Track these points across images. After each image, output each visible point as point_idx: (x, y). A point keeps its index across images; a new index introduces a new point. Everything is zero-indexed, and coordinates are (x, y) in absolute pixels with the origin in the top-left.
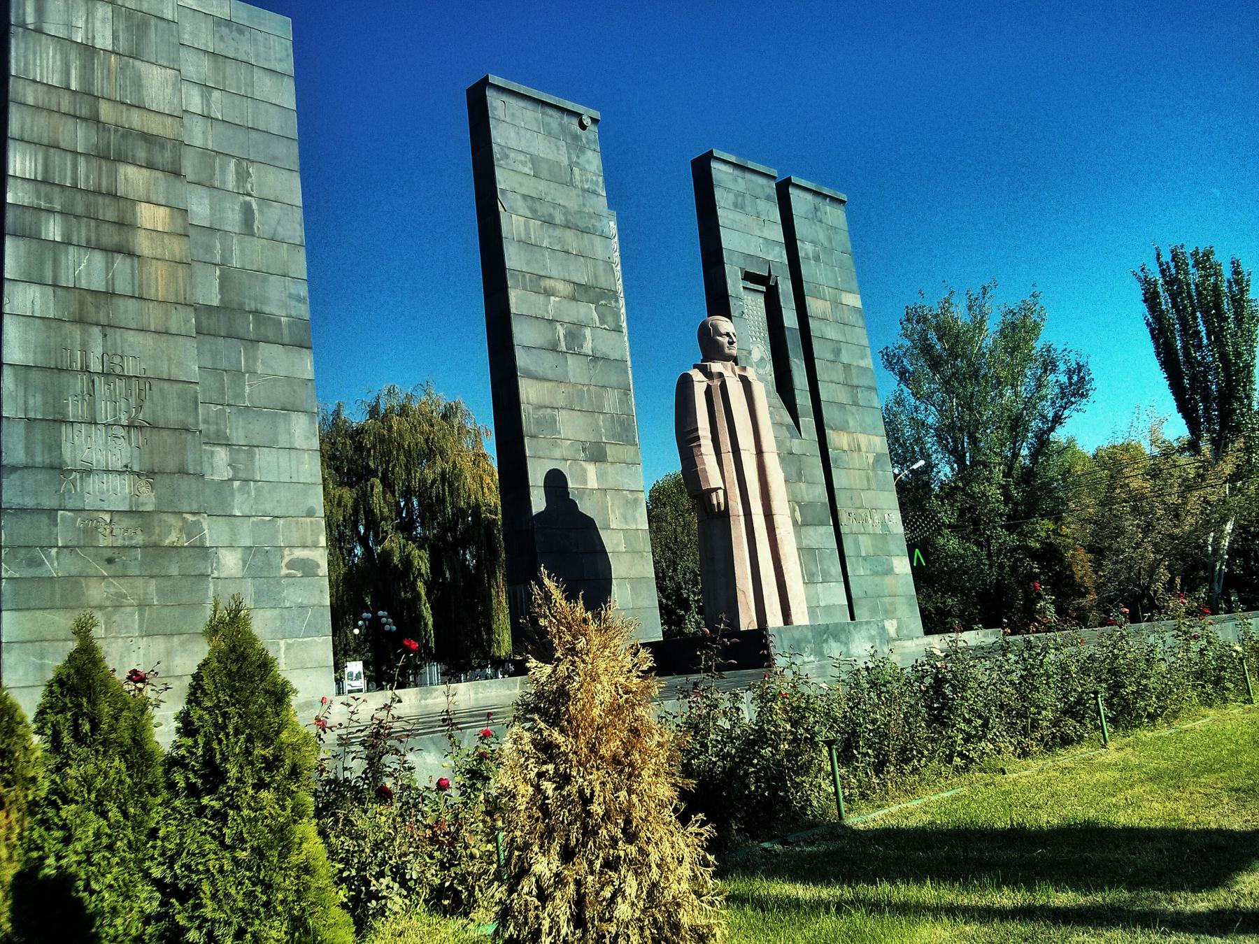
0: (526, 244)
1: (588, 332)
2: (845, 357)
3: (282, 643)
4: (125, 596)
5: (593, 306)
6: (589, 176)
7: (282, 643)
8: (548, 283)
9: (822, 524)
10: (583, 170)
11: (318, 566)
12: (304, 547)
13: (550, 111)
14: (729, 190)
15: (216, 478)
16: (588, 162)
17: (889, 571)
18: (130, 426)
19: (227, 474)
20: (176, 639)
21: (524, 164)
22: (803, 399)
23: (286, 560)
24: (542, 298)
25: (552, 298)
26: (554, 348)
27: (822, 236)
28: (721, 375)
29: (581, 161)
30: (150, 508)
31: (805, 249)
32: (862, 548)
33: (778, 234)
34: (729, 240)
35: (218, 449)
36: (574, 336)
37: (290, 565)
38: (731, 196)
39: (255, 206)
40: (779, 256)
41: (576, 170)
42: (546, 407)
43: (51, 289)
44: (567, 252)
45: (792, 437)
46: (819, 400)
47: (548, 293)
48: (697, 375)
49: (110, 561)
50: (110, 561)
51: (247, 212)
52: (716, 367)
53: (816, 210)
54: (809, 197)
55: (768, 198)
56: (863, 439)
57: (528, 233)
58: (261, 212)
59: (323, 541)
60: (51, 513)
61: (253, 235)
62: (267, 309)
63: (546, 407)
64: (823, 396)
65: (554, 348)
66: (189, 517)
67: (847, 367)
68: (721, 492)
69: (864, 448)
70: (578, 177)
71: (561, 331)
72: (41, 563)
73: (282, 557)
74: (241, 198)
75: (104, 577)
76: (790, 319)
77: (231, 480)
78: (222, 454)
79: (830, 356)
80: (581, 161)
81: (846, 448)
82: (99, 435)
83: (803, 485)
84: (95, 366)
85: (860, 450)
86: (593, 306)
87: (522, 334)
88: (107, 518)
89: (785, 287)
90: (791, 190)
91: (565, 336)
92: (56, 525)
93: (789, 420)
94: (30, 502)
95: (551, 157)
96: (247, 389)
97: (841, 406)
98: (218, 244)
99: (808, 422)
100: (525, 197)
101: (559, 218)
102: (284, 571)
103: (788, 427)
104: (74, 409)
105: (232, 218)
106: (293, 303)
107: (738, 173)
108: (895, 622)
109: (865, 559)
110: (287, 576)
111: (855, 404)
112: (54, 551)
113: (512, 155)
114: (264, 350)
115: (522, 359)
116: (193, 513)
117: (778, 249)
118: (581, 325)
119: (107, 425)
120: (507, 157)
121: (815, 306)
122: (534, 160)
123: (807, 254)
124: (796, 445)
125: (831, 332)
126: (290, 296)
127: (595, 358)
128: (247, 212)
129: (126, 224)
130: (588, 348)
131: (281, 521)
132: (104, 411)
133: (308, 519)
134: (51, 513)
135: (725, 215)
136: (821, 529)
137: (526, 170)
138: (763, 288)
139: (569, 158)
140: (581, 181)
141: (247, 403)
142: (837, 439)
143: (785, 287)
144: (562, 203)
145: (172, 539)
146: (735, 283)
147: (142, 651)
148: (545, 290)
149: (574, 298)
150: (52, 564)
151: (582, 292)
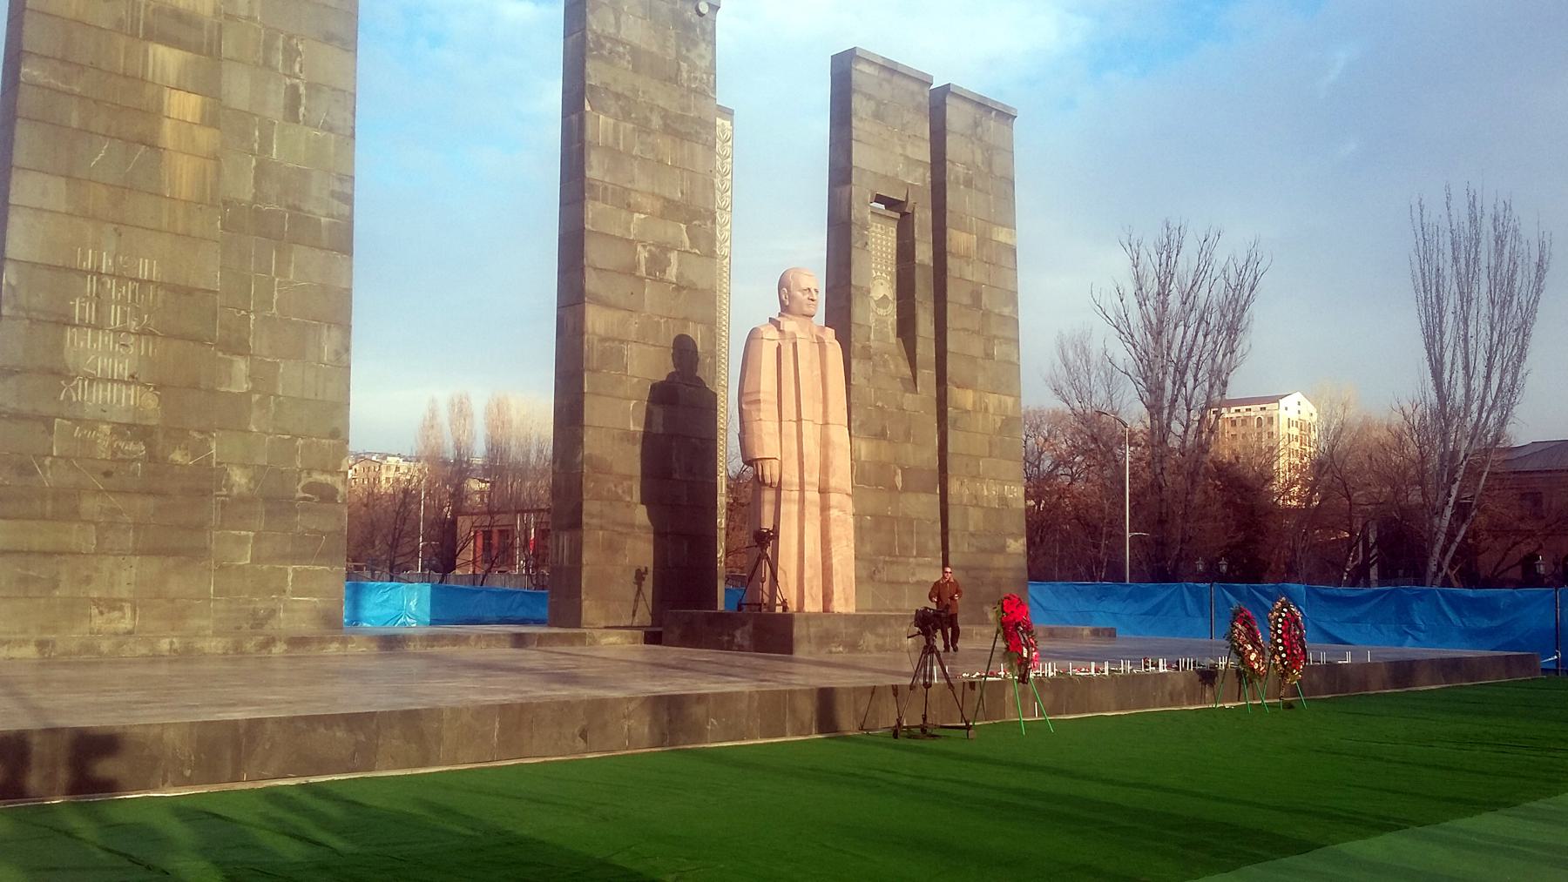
0: (614, 153)
1: (673, 256)
4: (120, 512)
5: (683, 226)
6: (698, 74)
9: (926, 491)
10: (693, 68)
11: (337, 491)
12: (324, 471)
14: (869, 97)
15: (234, 390)
16: (702, 57)
17: (1002, 549)
18: (139, 334)
19: (246, 387)
20: (171, 561)
22: (925, 349)
24: (624, 214)
26: (630, 270)
27: (979, 158)
28: (794, 336)
29: (692, 55)
30: (153, 422)
31: (955, 171)
32: (971, 523)
33: (924, 153)
34: (862, 156)
36: (657, 264)
37: (309, 488)
38: (872, 104)
39: (302, 90)
40: (920, 178)
41: (684, 66)
42: (614, 340)
43: (63, 180)
44: (660, 162)
45: (906, 390)
46: (945, 351)
47: (630, 208)
48: (772, 333)
50: (107, 474)
52: (789, 325)
53: (976, 124)
54: (968, 107)
55: (918, 108)
56: (992, 400)
57: (616, 139)
58: (308, 97)
60: (47, 421)
61: (298, 122)
62: (306, 207)
63: (614, 340)
64: (950, 346)
66: (195, 434)
67: (987, 314)
68: (775, 463)
69: (991, 410)
70: (685, 75)
71: (643, 255)
73: (299, 480)
74: (288, 81)
76: (924, 253)
77: (248, 394)
78: (241, 366)
79: (966, 300)
80: (692, 55)
81: (969, 407)
82: (105, 339)
83: (910, 447)
84: (106, 264)
85: (986, 409)
86: (683, 226)
87: (594, 253)
88: (106, 428)
89: (923, 217)
90: (948, 100)
92: (51, 433)
93: (907, 372)
94: (26, 408)
95: (654, 49)
97: (973, 359)
99: (927, 374)
100: (618, 96)
101: (656, 121)
102: (300, 494)
103: (903, 380)
104: (81, 308)
105: (276, 103)
106: (336, 202)
107: (884, 75)
109: (972, 535)
110: (305, 499)
111: (989, 356)
112: (48, 461)
113: (608, 45)
114: (299, 254)
115: (592, 283)
116: (201, 432)
117: (921, 170)
118: (664, 248)
119: (115, 331)
120: (602, 46)
121: (958, 239)
123: (957, 178)
124: (909, 400)
125: (972, 273)
126: (333, 194)
127: (679, 288)
129: (154, 113)
130: (672, 273)
131: (300, 442)
132: (115, 315)
134: (47, 421)
135: (861, 126)
136: (924, 498)
138: (897, 216)
139: (678, 52)
140: (689, 79)
142: (962, 398)
143: (923, 217)
144: (661, 103)
145: (177, 456)
146: (864, 209)
147: (134, 570)
148: (629, 205)
149: (662, 216)
150: (44, 473)
151: (671, 210)
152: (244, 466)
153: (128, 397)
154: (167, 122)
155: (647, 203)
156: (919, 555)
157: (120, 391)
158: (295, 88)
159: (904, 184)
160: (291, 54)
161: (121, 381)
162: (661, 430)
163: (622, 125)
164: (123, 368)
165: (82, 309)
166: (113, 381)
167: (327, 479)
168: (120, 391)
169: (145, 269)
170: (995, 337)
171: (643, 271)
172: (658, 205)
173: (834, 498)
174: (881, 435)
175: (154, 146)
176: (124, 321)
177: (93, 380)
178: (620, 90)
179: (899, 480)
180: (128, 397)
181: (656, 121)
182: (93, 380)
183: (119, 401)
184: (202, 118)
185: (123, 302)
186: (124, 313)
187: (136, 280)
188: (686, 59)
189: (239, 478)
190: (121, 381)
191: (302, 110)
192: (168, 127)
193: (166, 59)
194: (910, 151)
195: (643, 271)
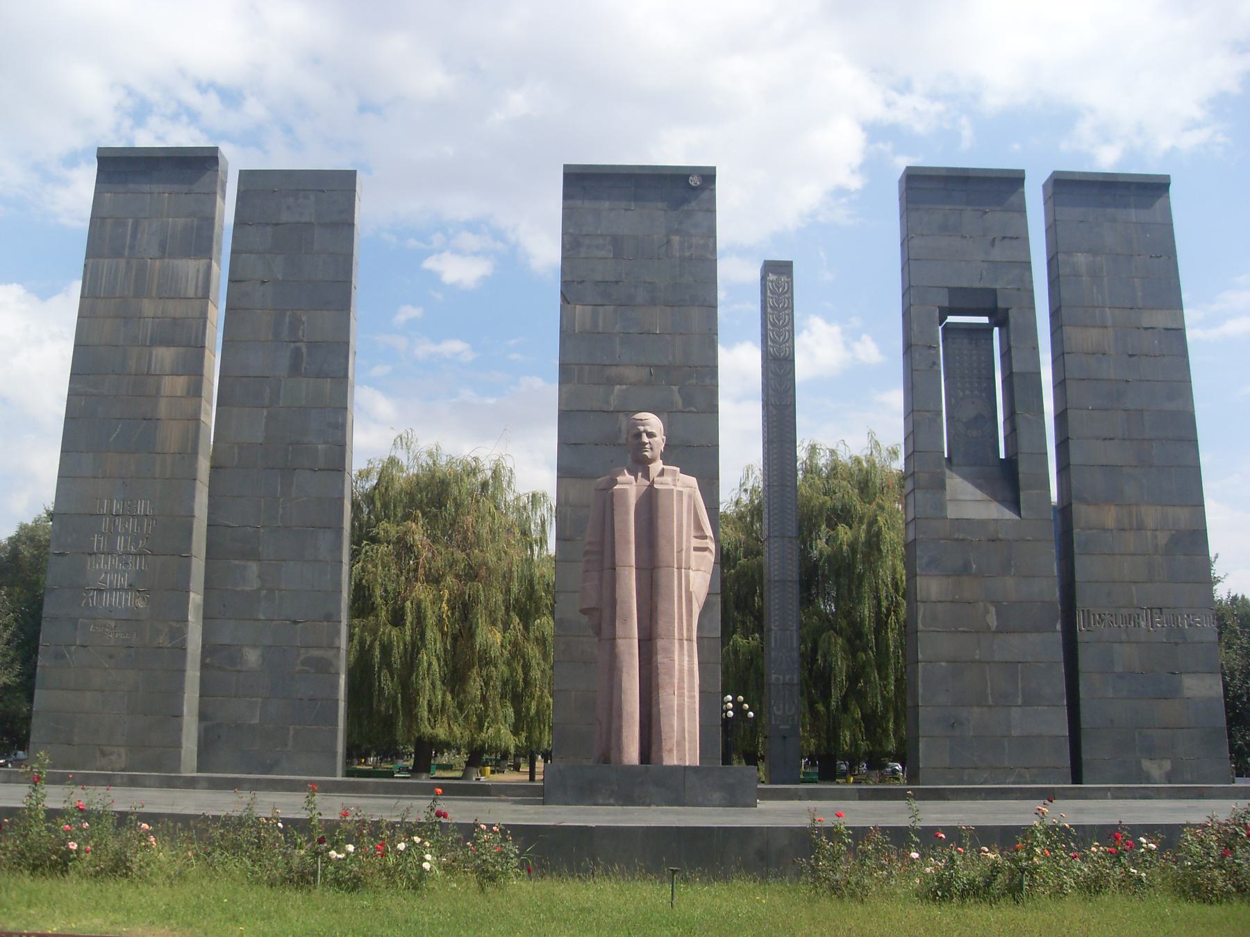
3: (291, 728)
5: (675, 388)
7: (291, 728)
8: (613, 371)
15: (247, 588)
19: (256, 584)
23: (302, 658)
25: (617, 387)
35: (250, 563)
39: (304, 350)
41: (676, 239)
47: (611, 382)
49: (111, 657)
56: (1151, 515)
66: (174, 624)
72: (63, 657)
74: (292, 345)
75: (106, 669)
78: (253, 567)
85: (1141, 527)
88: (113, 624)
96: (281, 511)
98: (268, 390)
100: (597, 283)
102: (299, 668)
104: (98, 542)
122: (616, 241)
132: (120, 541)
133: (325, 623)
141: (279, 524)
152: (255, 646)
153: (126, 600)
155: (631, 373)
156: (1026, 703)
157: (121, 597)
158: (298, 350)
159: (993, 292)
161: (122, 589)
163: (601, 309)
164: (124, 581)
165: (99, 541)
166: (116, 590)
168: (121, 597)
169: (140, 510)
172: (644, 373)
174: (965, 570)
175: (152, 420)
176: (125, 547)
177: (100, 591)
178: (599, 278)
179: (992, 620)
180: (126, 600)
183: (120, 603)
184: (188, 393)
185: (126, 534)
186: (126, 541)
187: (137, 516)
188: (677, 232)
189: (252, 657)
190: (122, 589)
191: (304, 365)
192: (163, 405)
193: (165, 356)
194: (997, 254)
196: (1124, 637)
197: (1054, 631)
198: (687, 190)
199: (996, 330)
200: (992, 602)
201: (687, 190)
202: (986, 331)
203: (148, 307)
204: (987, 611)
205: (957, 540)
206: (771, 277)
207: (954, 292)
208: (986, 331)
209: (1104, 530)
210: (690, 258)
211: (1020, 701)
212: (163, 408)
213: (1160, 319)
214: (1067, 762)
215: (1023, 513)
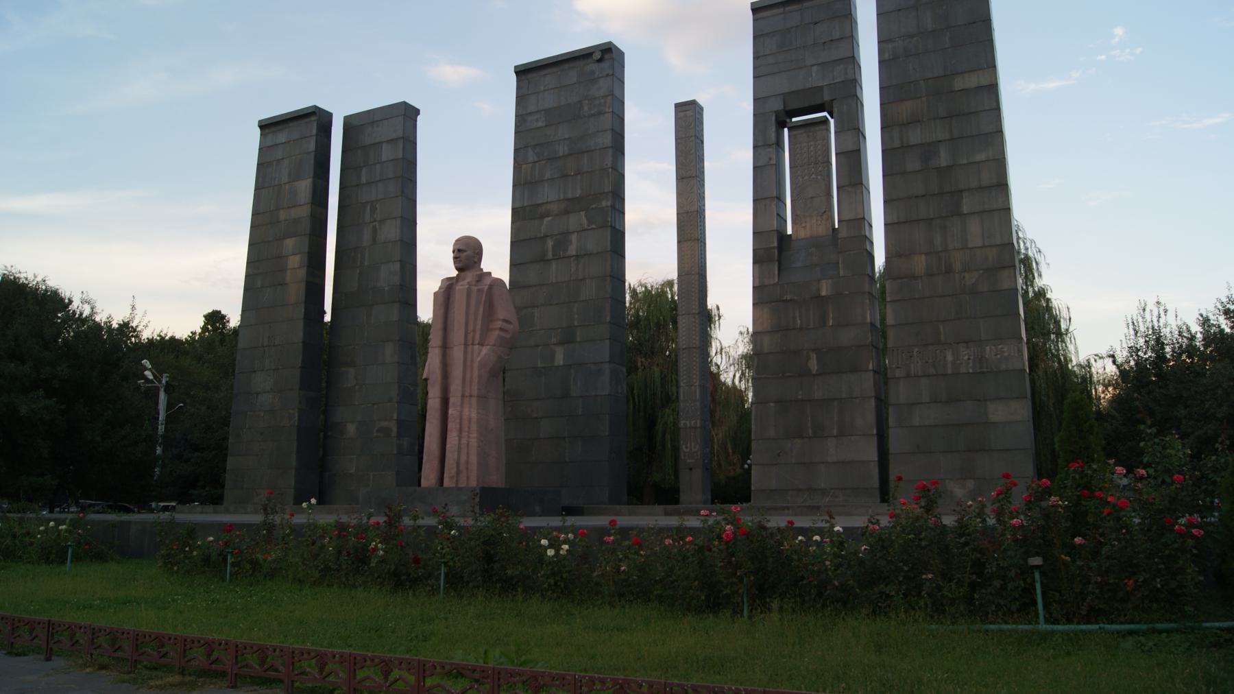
1: (574, 237)
2: (944, 159)
5: (583, 213)
13: (566, 66)
21: (537, 120)
44: (565, 176)
47: (542, 217)
51: (375, 230)
59: (395, 417)
65: (542, 260)
70: (586, 108)
78: (352, 371)
85: (949, 270)
91: (553, 247)
101: (562, 150)
108: (970, 484)
111: (958, 213)
128: (375, 230)
130: (572, 250)
137: (540, 124)
149: (566, 212)
154: (288, 273)
159: (821, 89)
160: (374, 210)
162: (561, 363)
167: (385, 424)
170: (961, 191)
171: (550, 255)
173: (452, 400)
175: (283, 284)
177: (258, 394)
179: (813, 365)
181: (562, 150)
182: (258, 394)
189: (351, 429)
193: (290, 243)
195: (550, 255)
196: (932, 371)
197: (867, 370)
198: (602, 63)
199: (832, 121)
200: (813, 350)
201: (602, 63)
202: (824, 121)
203: (283, 215)
204: (808, 358)
205: (786, 301)
206: (682, 114)
207: (785, 97)
208: (824, 121)
209: (915, 277)
210: (594, 115)
211: (835, 432)
212: (289, 277)
213: (972, 81)
214: (875, 482)
215: (842, 273)
